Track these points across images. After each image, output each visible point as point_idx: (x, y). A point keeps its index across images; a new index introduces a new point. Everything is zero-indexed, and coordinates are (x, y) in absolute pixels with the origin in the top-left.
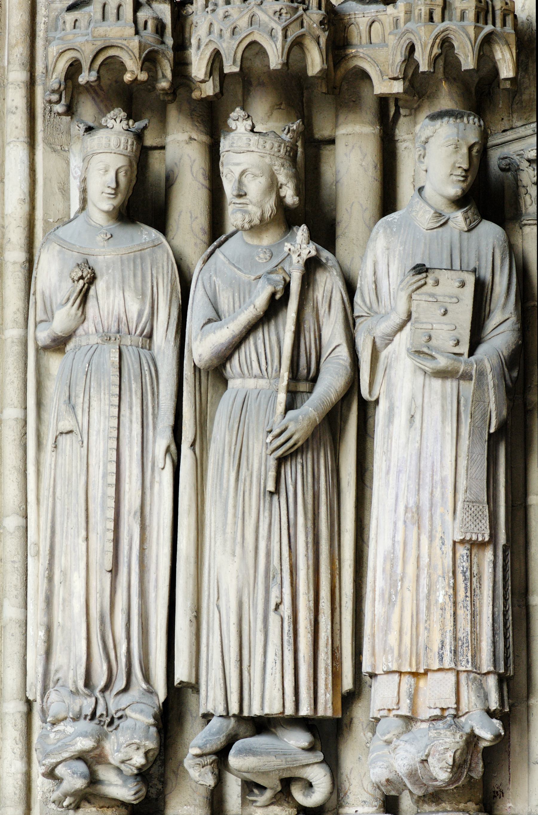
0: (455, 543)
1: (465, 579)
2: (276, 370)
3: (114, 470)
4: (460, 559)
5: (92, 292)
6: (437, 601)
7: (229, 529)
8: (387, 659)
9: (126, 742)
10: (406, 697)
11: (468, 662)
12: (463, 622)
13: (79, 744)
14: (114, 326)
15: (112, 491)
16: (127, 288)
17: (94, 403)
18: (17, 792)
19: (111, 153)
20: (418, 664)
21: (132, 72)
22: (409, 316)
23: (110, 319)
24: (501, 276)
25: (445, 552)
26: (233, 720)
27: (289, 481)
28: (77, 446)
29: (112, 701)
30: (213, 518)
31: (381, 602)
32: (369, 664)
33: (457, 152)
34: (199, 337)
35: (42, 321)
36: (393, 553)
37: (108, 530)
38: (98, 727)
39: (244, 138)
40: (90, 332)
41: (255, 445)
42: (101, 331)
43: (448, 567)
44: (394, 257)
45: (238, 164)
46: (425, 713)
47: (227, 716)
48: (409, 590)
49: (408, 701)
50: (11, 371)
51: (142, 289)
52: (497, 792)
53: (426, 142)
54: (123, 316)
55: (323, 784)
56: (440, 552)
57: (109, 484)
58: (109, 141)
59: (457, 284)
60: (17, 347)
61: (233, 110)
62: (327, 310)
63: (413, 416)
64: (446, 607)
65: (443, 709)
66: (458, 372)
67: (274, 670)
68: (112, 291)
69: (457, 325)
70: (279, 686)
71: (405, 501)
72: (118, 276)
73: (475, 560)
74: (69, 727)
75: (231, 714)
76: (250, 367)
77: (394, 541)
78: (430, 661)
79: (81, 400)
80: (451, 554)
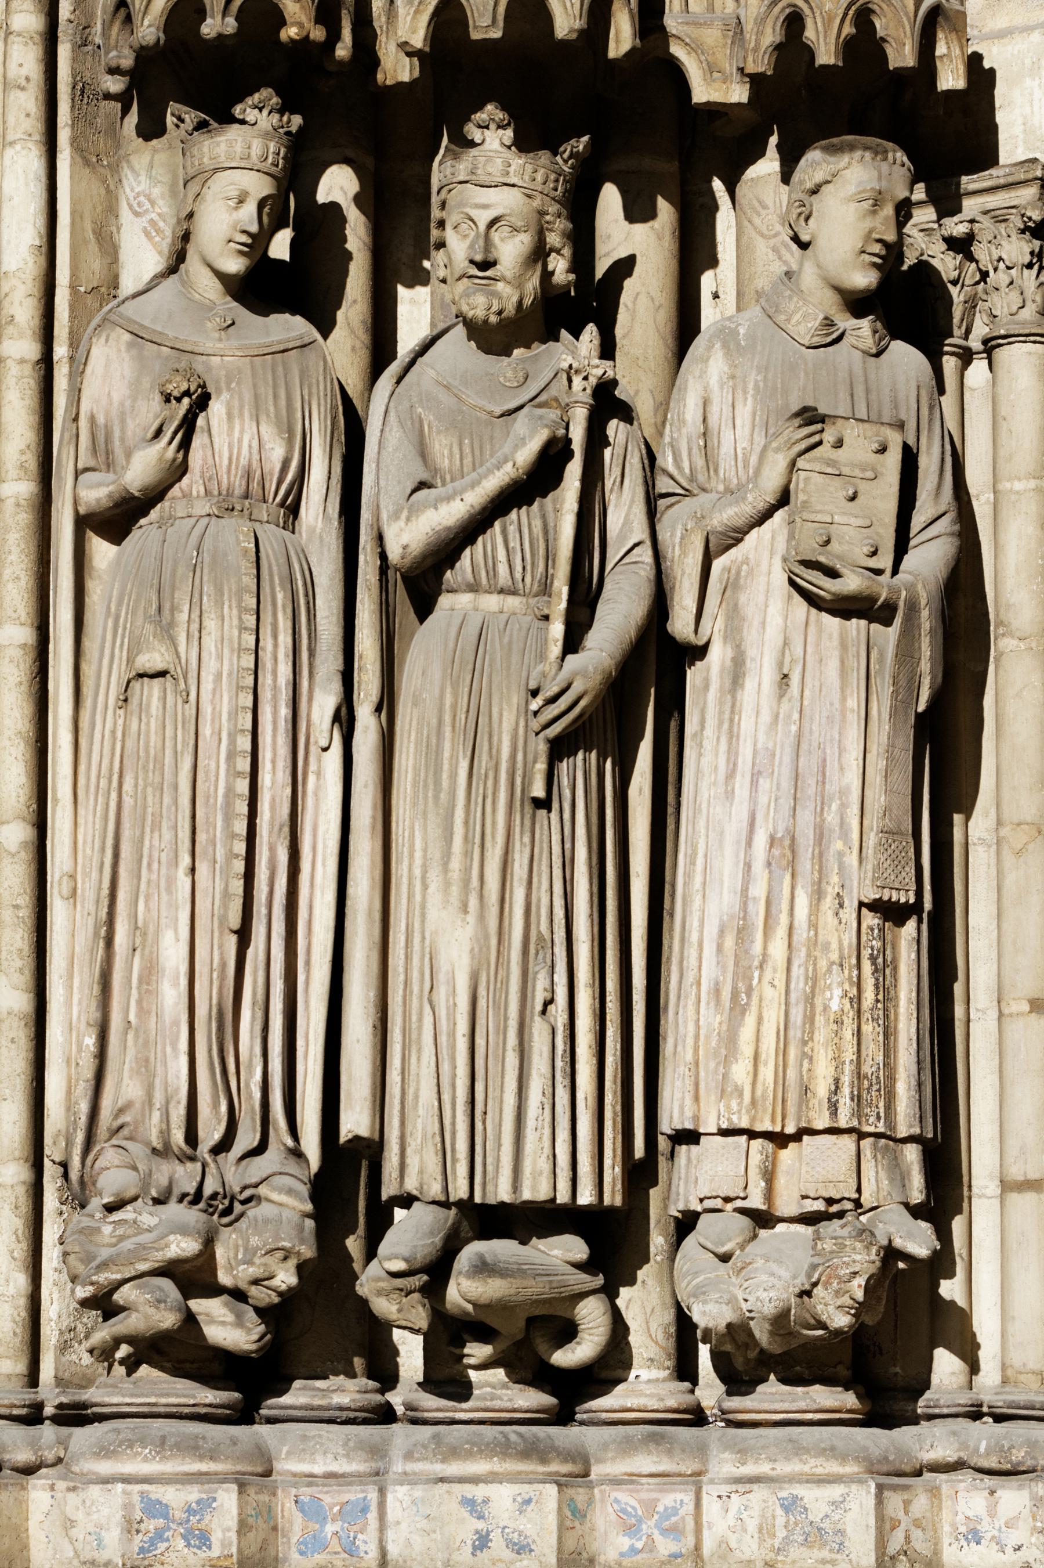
0: (861, 904)
1: (876, 971)
2: (539, 581)
4: (868, 934)
5: (200, 421)
6: (826, 1008)
8: (728, 1107)
9: (264, 1246)
10: (760, 1176)
11: (878, 1118)
12: (872, 1046)
13: (173, 1247)
14: (240, 485)
15: (243, 786)
16: (263, 419)
17: (211, 624)
18: (18, 1331)
19: (251, 169)
21: (300, 25)
22: (784, 499)
23: (233, 472)
24: (930, 437)
25: (844, 921)
26: (454, 1211)
27: (565, 781)
31: (712, 1005)
33: (874, 212)
34: (405, 513)
35: (86, 470)
36: (744, 918)
37: (237, 856)
39: (499, 161)
40: (195, 493)
41: (505, 714)
42: (216, 493)
44: (745, 392)
45: (485, 207)
46: (787, 1205)
47: (445, 1204)
48: (774, 986)
49: (763, 1184)
50: (13, 557)
51: (289, 421)
54: (255, 464)
55: (601, 1329)
56: (836, 921)
57: (239, 773)
58: (249, 148)
59: (875, 446)
60: (25, 515)
61: (480, 107)
62: (619, 479)
63: (786, 676)
64: (845, 1018)
65: (830, 1201)
66: (876, 601)
67: (540, 1122)
69: (874, 519)
70: (547, 1150)
71: (771, 826)
72: (248, 396)
73: (889, 937)
75: (452, 1200)
76: (491, 573)
77: (747, 896)
78: (811, 1114)
79: (184, 616)
80: (855, 925)
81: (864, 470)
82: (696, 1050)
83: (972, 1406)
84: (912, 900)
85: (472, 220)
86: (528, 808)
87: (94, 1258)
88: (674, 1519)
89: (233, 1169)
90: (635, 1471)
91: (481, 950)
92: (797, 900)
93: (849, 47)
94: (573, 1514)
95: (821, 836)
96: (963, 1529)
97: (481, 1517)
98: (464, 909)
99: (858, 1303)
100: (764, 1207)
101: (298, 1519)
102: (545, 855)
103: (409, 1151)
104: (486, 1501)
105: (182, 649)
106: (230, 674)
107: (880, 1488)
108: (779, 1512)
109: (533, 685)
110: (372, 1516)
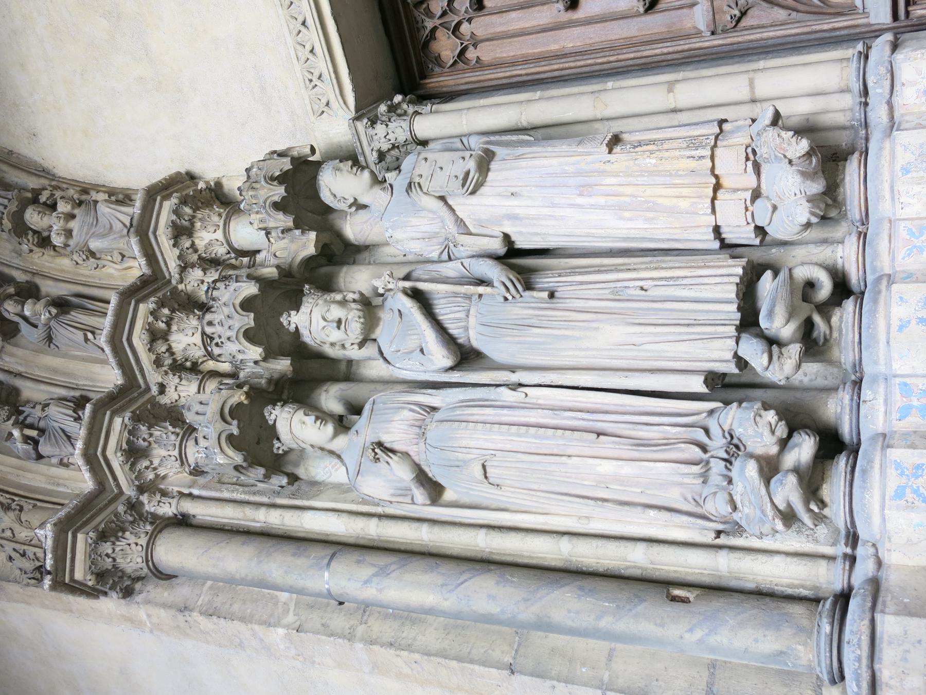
1: (640, 145)
6: (655, 165)
7: (577, 333)
11: (708, 139)
13: (752, 474)
15: (532, 430)
17: (464, 443)
21: (241, 394)
22: (442, 198)
30: (571, 353)
34: (430, 357)
35: (412, 499)
38: (739, 459)
41: (515, 312)
46: (752, 181)
53: (335, 196)
59: (423, 162)
61: (281, 324)
65: (747, 159)
68: (391, 430)
70: (712, 287)
85: (324, 328)
86: (554, 300)
87: (761, 518)
88: (914, 230)
89: (714, 442)
90: (887, 250)
93: (280, 183)
95: (579, 173)
97: (909, 322)
98: (597, 329)
99: (794, 135)
101: (909, 419)
102: (575, 292)
106: (484, 434)
108: (909, 175)
109: (502, 300)
110: (908, 381)
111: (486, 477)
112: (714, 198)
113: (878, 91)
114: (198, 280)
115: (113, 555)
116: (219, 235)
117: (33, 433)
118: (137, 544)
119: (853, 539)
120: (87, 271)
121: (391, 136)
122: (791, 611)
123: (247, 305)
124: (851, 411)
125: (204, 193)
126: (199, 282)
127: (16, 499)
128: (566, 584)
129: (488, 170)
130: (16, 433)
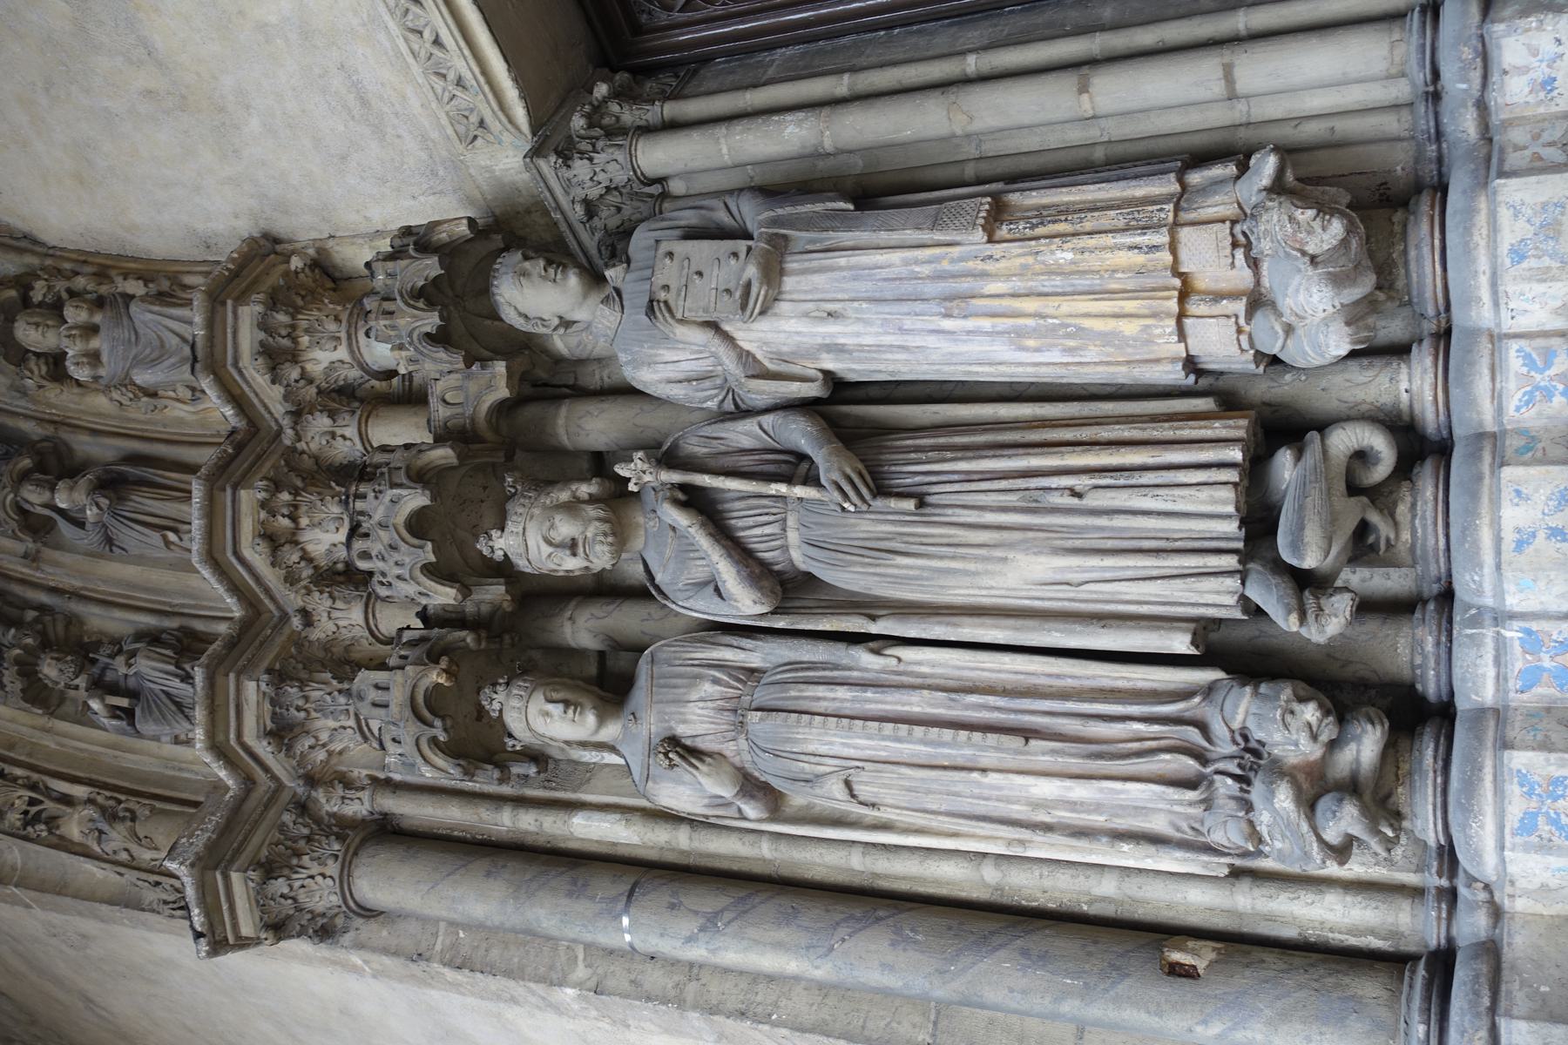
0: (990, 241)
1: (1042, 223)
3: (891, 725)
5: (688, 742)
6: (1073, 262)
7: (971, 566)
8: (1160, 336)
12: (1102, 221)
15: (919, 731)
16: (687, 698)
17: (811, 748)
20: (1167, 289)
26: (1251, 566)
28: (864, 776)
29: (1219, 749)
30: (962, 592)
32: (1169, 367)
36: (1009, 333)
37: (969, 738)
43: (1022, 247)
44: (656, 355)
46: (1242, 277)
50: (808, 856)
52: (1381, 195)
53: (526, 317)
56: (1003, 260)
59: (667, 261)
61: (480, 552)
63: (829, 314)
65: (1235, 245)
72: (672, 708)
74: (1262, 818)
75: (1240, 567)
79: (806, 765)
80: (1005, 245)
81: (683, 268)
82: (1118, 363)
83: (1427, 101)
84: (989, 199)
85: (550, 556)
88: (1534, 356)
89: (1219, 749)
90: (1489, 394)
91: (1037, 546)
92: (992, 292)
93: (431, 305)
94: (1529, 450)
96: (1542, 95)
97: (1534, 535)
98: (1005, 560)
99: (1318, 215)
100: (1245, 300)
101: (1539, 690)
103: (1201, 601)
104: (1518, 530)
105: (828, 769)
107: (1502, 174)
108: (1525, 265)
109: (839, 510)
110: (1534, 626)
111: (853, 796)
112: (1181, 316)
113: (1458, 83)
114: (325, 433)
115: (292, 894)
116: (342, 353)
117: (124, 702)
118: (324, 876)
119: (1448, 856)
120: (139, 414)
121: (601, 177)
122: (1360, 993)
123: (418, 525)
124: (1438, 663)
125: (302, 276)
126: (328, 438)
127: (123, 797)
128: (1001, 946)
129: (782, 272)
130: (95, 705)
